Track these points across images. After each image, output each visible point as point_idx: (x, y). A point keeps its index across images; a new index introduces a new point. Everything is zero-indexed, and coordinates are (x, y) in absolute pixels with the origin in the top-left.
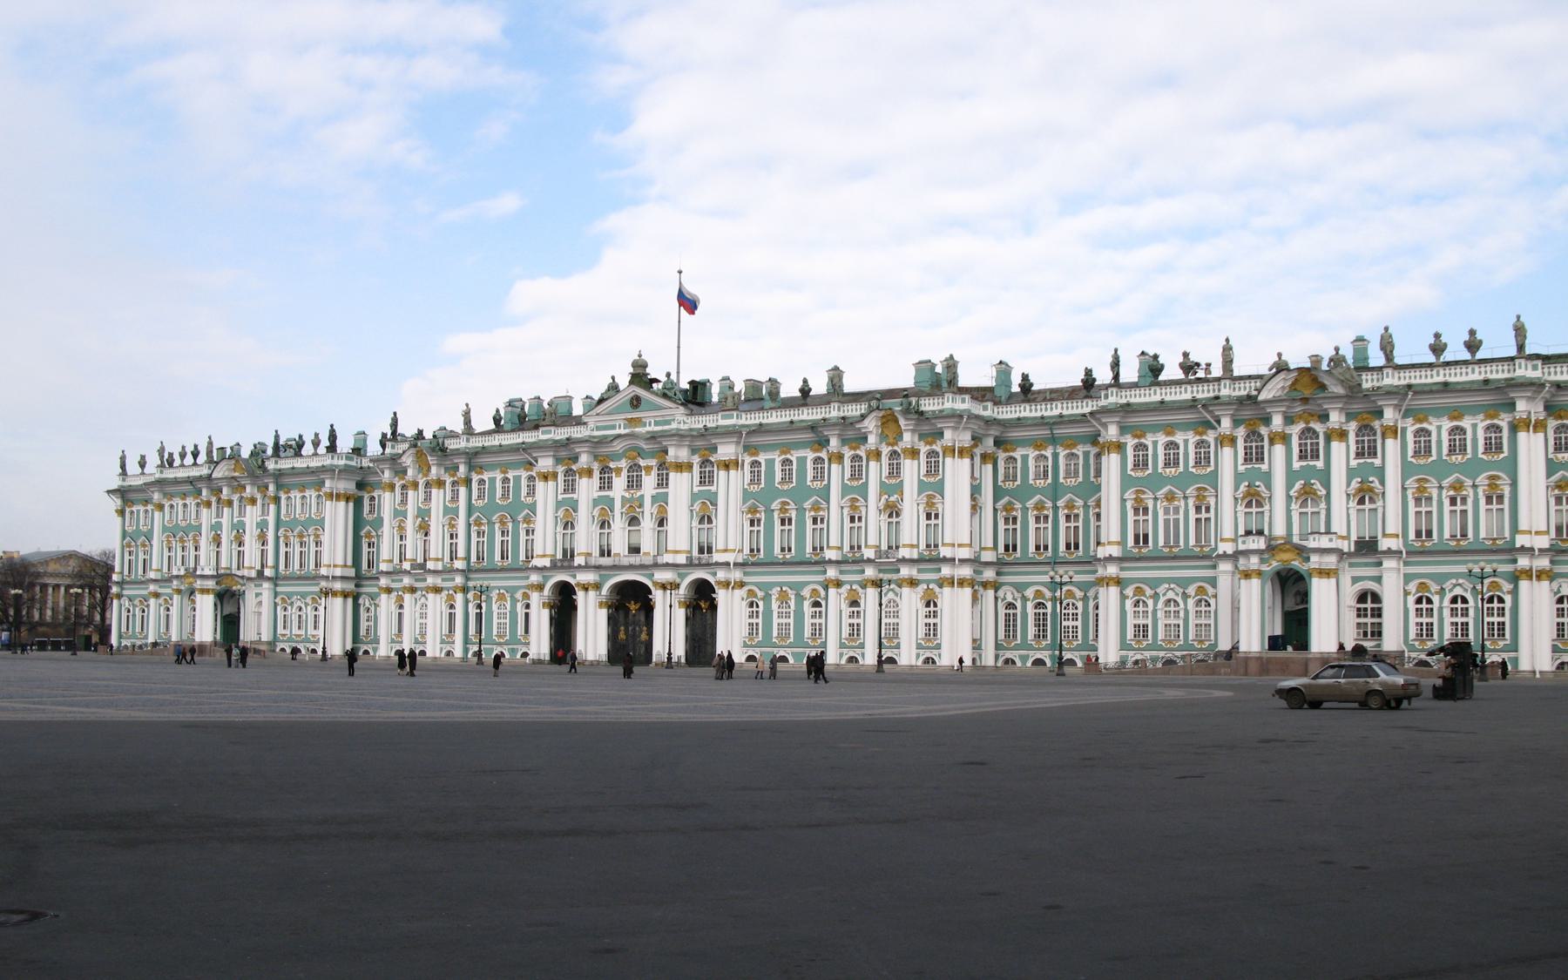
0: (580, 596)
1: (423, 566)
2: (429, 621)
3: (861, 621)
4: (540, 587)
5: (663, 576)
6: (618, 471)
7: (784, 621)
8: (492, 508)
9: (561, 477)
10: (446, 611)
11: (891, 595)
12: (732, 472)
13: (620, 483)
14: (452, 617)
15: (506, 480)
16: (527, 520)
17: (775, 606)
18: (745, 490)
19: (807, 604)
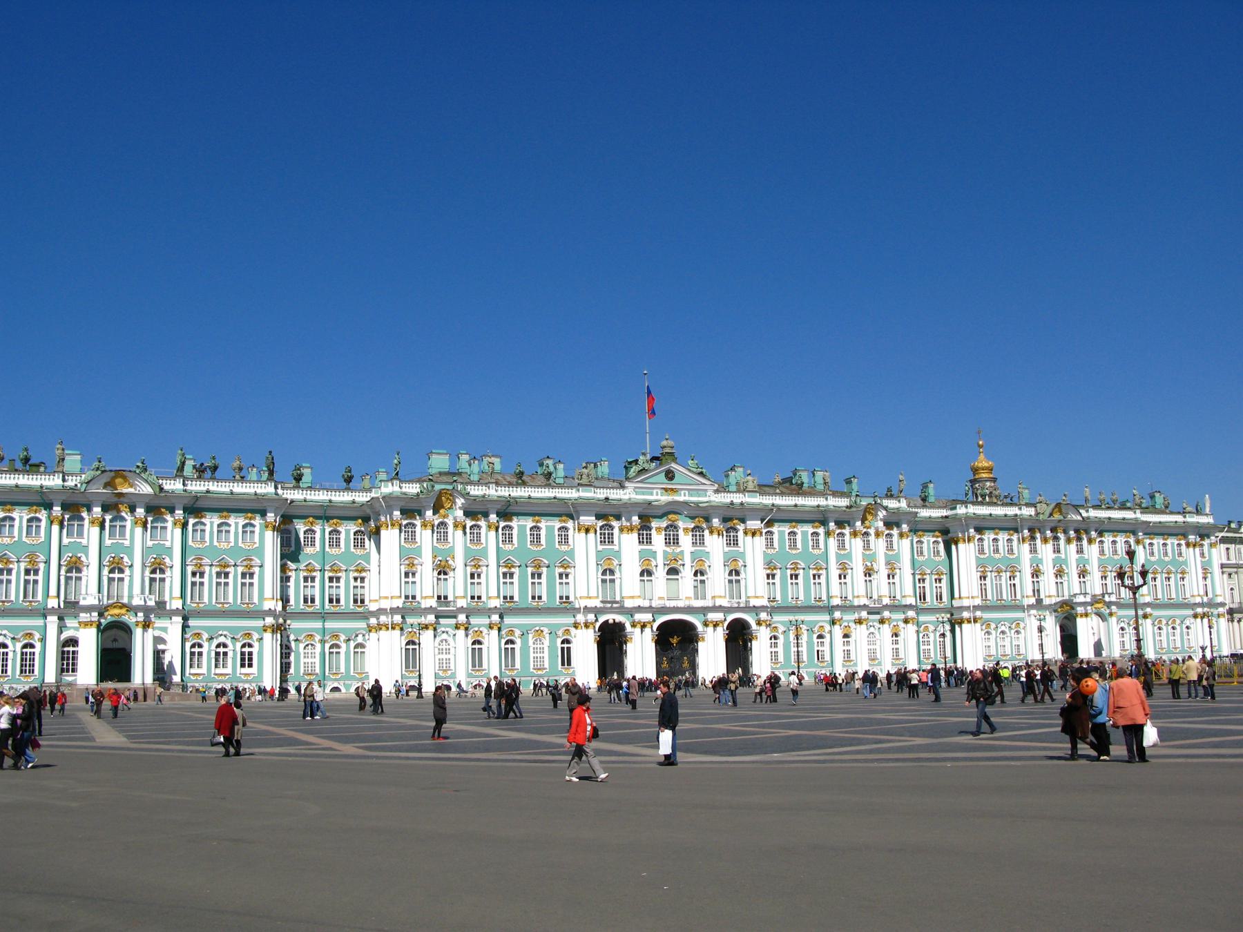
6: (658, 529)
11: (872, 630)
12: (757, 538)
13: (658, 539)
19: (815, 636)
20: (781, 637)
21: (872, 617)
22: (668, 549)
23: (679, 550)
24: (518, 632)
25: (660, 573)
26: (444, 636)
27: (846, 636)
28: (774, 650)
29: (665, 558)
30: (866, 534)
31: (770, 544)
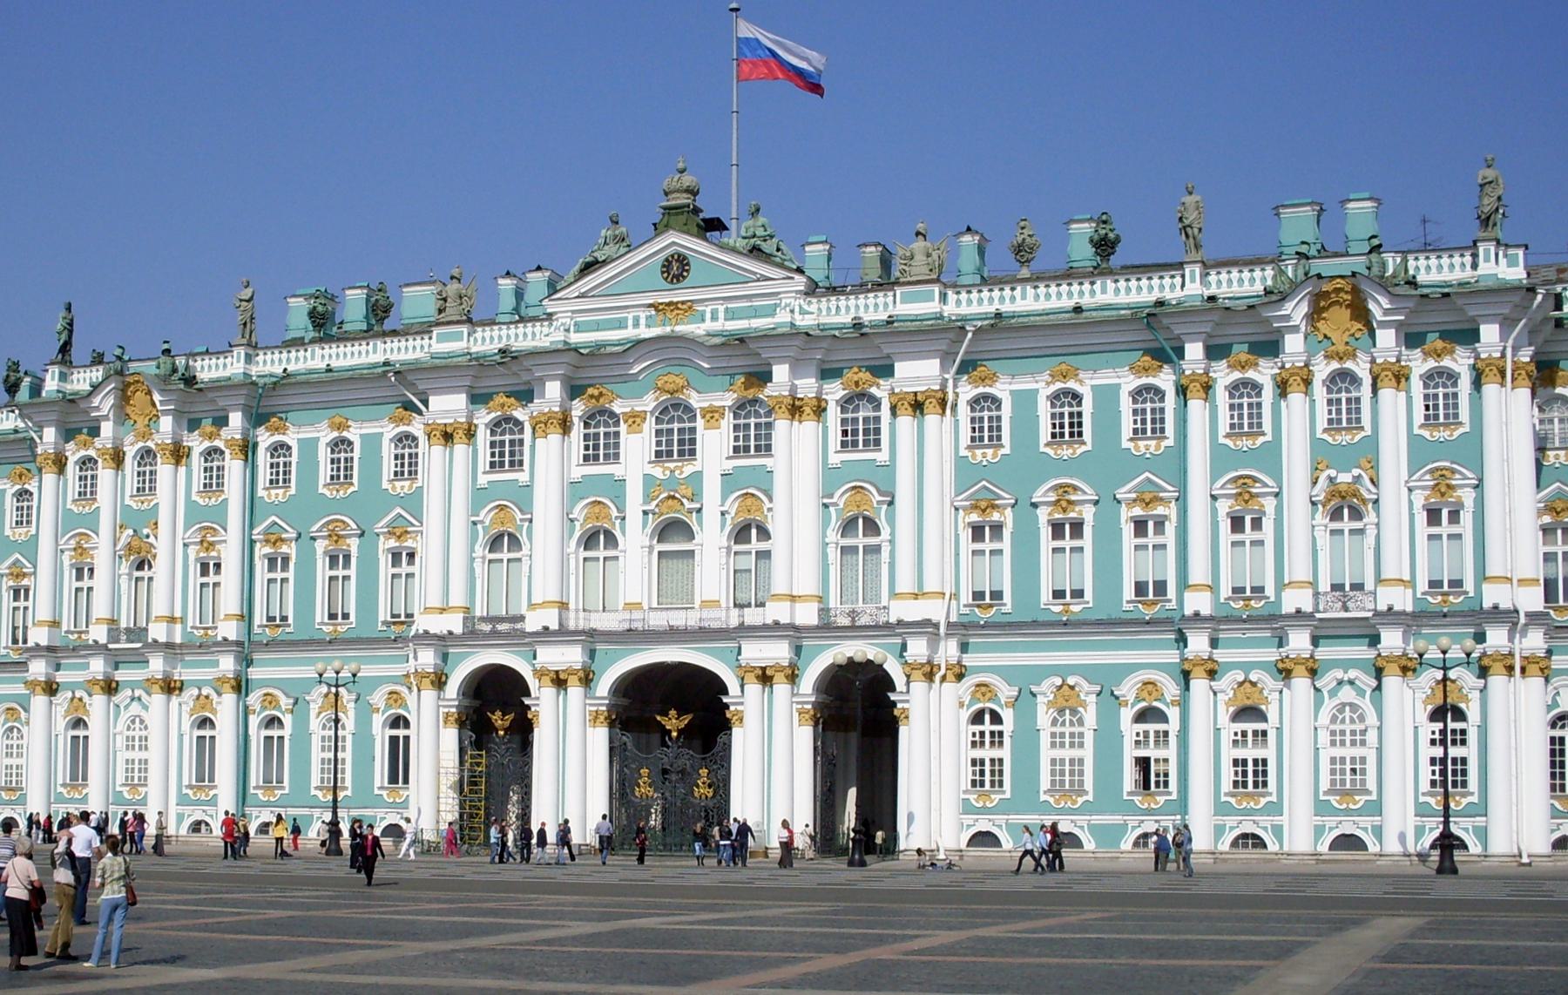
0: (542, 700)
1: (137, 633)
2: (154, 755)
3: (1269, 753)
4: (439, 682)
5: (758, 652)
6: (635, 419)
7: (1067, 753)
8: (308, 505)
9: (483, 436)
10: (191, 735)
11: (1347, 694)
12: (931, 419)
13: (637, 447)
14: (205, 748)
15: (340, 444)
16: (398, 531)
17: (1044, 717)
18: (960, 461)
19: (1127, 714)
20: (1007, 715)
21: (1325, 652)
22: (657, 472)
23: (688, 469)
24: (285, 702)
25: (635, 538)
26: (135, 708)
27: (1249, 712)
28: (987, 753)
29: (648, 498)
30: (1343, 378)
31: (985, 433)
